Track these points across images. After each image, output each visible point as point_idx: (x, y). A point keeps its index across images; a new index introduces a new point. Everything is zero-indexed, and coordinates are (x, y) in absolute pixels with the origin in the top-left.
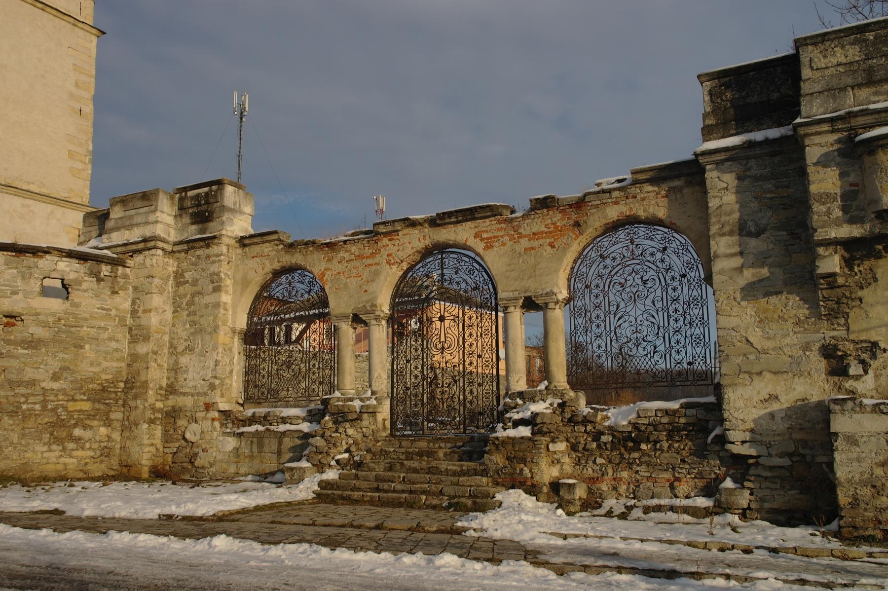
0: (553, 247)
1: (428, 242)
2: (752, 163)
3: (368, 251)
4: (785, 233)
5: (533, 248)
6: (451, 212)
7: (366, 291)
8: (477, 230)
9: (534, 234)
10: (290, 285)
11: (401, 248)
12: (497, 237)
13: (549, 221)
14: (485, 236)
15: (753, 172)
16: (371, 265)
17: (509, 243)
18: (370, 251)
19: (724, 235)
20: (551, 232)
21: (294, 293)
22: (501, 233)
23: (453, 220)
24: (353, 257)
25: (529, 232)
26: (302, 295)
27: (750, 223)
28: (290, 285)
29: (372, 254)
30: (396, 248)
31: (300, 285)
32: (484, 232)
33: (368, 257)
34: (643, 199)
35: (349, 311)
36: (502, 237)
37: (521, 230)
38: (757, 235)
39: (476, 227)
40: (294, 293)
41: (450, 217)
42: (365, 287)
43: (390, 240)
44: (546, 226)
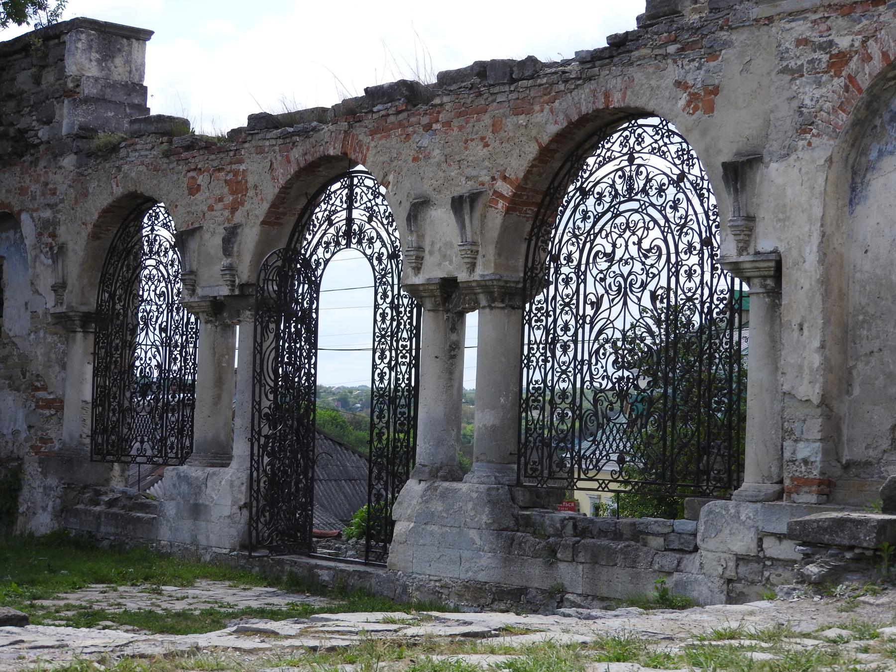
10: (631, 160)
21: (640, 183)
26: (661, 190)
28: (631, 160)
31: (656, 161)
40: (640, 183)
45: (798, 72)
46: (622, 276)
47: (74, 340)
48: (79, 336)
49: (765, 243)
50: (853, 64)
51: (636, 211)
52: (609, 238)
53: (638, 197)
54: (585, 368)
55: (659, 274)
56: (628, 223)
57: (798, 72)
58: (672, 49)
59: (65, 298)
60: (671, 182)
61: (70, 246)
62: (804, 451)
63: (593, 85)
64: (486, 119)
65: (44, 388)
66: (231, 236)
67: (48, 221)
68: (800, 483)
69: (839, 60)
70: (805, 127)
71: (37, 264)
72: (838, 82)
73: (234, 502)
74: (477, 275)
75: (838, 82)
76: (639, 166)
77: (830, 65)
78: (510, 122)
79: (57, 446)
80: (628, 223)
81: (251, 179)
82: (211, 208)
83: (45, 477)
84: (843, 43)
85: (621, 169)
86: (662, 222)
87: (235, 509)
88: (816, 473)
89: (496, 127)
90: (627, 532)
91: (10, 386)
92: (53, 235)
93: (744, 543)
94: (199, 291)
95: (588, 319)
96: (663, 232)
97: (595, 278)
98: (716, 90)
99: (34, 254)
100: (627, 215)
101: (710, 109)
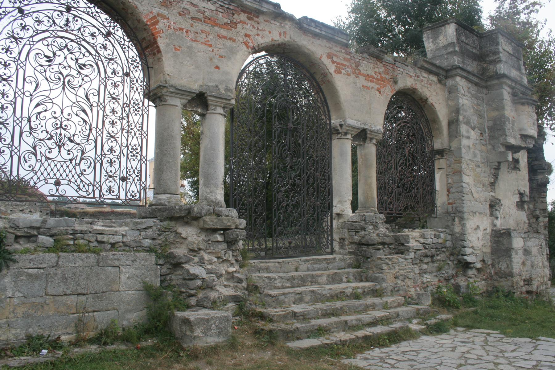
0: (380, 92)
1: (287, 39)
2: (470, 85)
3: (222, 18)
4: (480, 132)
5: (368, 88)
6: (318, 22)
7: (217, 68)
8: (329, 51)
9: (368, 75)
10: (69, 9)
11: (260, 33)
12: (344, 65)
13: (376, 70)
14: (335, 59)
15: (470, 90)
16: (225, 37)
17: (353, 76)
18: (226, 20)
19: (464, 123)
20: (378, 80)
22: (347, 64)
23: (317, 31)
24: (201, 16)
25: (365, 72)
27: (472, 121)
28: (69, 9)
29: (226, 24)
30: (255, 32)
32: (335, 55)
33: (220, 26)
34: (422, 81)
35: (195, 87)
36: (348, 67)
37: (360, 68)
38: (473, 129)
39: (330, 48)
41: (316, 27)
42: (216, 61)
43: (249, 19)
44: (375, 73)
46: (61, 73)
51: (73, 41)
52: (50, 48)
53: (73, 32)
54: (25, 122)
55: (91, 81)
56: (66, 45)
60: (101, 33)
76: (75, 16)
80: (66, 45)
85: (61, 12)
86: (93, 52)
95: (27, 94)
96: (94, 59)
97: (35, 69)
100: (67, 41)
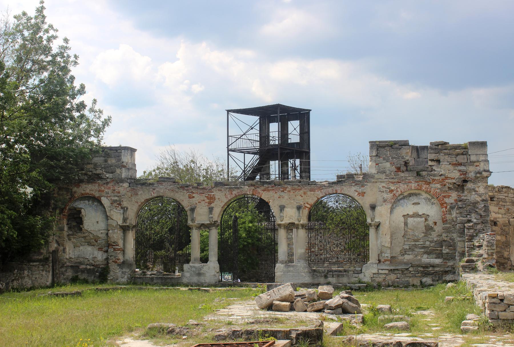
45: (383, 192)
47: (129, 232)
48: (130, 231)
49: (377, 220)
50: (395, 192)
57: (383, 192)
58: (353, 184)
59: (128, 221)
61: (129, 208)
62: (386, 255)
63: (332, 188)
64: (302, 191)
65: (118, 245)
66: (211, 210)
67: (116, 200)
68: (386, 260)
69: (391, 191)
70: (385, 201)
71: (112, 212)
72: (392, 195)
73: (216, 271)
74: (301, 222)
75: (392, 195)
77: (389, 192)
78: (309, 193)
79: (122, 261)
81: (217, 197)
82: (200, 202)
83: (122, 269)
84: (393, 188)
87: (216, 273)
88: (389, 259)
89: (305, 193)
90: (343, 271)
91: (88, 244)
92: (120, 204)
93: (375, 271)
94: (196, 222)
98: (365, 193)
99: (110, 209)
101: (363, 196)
